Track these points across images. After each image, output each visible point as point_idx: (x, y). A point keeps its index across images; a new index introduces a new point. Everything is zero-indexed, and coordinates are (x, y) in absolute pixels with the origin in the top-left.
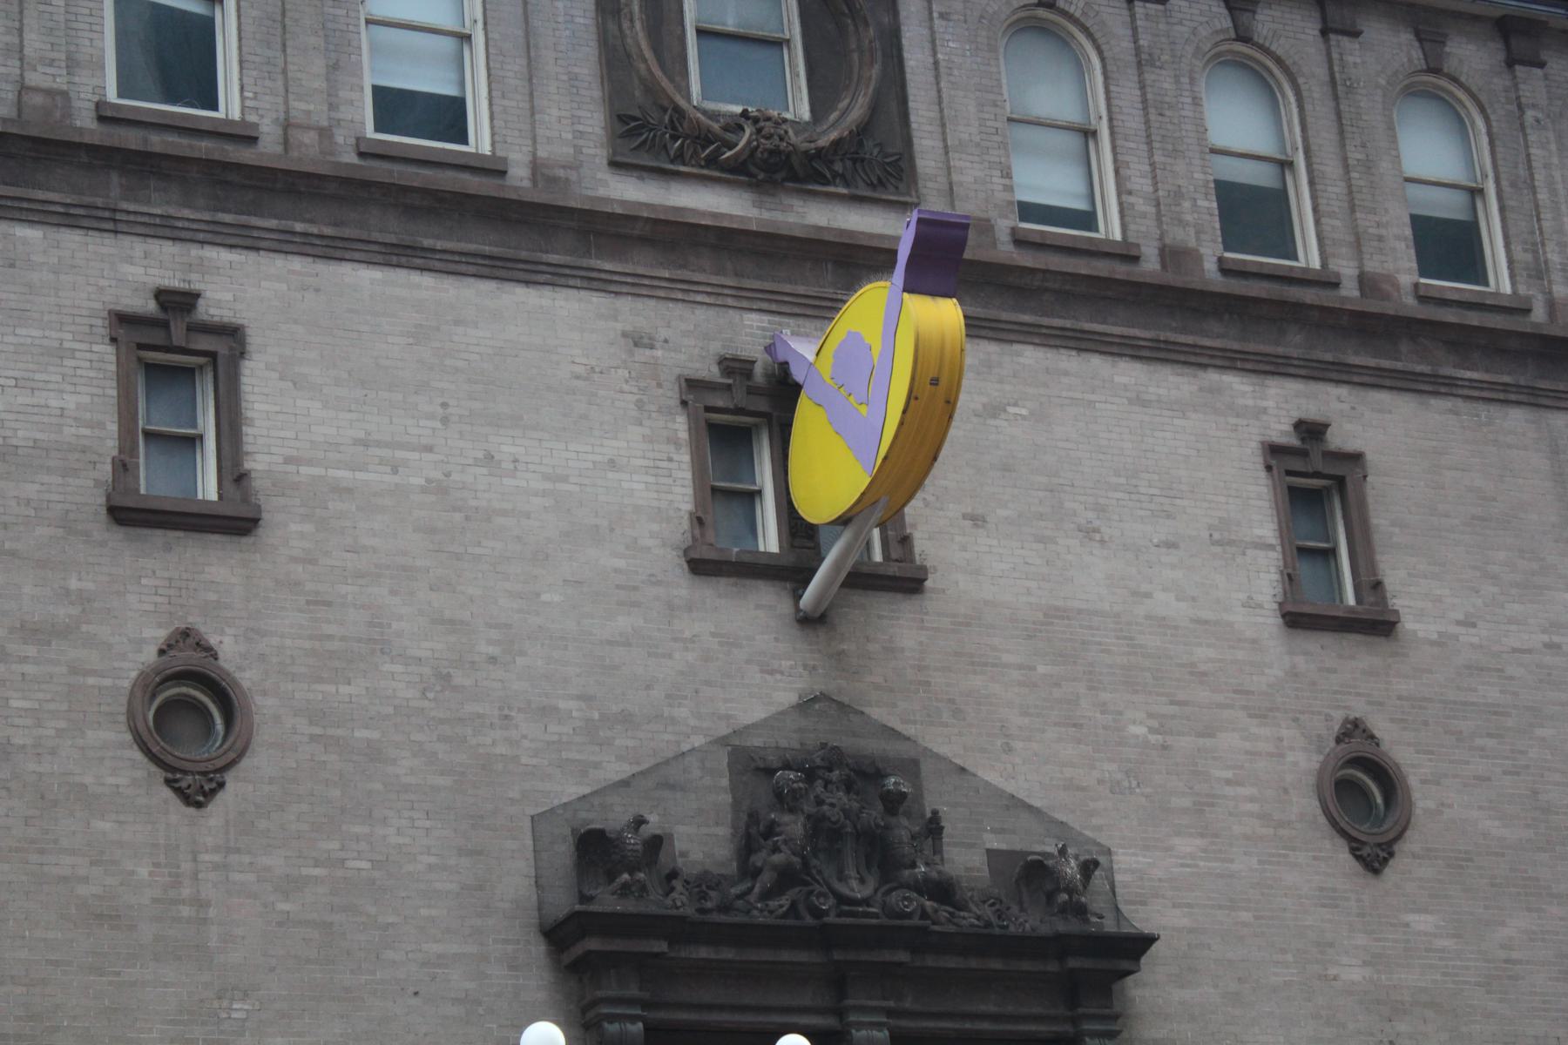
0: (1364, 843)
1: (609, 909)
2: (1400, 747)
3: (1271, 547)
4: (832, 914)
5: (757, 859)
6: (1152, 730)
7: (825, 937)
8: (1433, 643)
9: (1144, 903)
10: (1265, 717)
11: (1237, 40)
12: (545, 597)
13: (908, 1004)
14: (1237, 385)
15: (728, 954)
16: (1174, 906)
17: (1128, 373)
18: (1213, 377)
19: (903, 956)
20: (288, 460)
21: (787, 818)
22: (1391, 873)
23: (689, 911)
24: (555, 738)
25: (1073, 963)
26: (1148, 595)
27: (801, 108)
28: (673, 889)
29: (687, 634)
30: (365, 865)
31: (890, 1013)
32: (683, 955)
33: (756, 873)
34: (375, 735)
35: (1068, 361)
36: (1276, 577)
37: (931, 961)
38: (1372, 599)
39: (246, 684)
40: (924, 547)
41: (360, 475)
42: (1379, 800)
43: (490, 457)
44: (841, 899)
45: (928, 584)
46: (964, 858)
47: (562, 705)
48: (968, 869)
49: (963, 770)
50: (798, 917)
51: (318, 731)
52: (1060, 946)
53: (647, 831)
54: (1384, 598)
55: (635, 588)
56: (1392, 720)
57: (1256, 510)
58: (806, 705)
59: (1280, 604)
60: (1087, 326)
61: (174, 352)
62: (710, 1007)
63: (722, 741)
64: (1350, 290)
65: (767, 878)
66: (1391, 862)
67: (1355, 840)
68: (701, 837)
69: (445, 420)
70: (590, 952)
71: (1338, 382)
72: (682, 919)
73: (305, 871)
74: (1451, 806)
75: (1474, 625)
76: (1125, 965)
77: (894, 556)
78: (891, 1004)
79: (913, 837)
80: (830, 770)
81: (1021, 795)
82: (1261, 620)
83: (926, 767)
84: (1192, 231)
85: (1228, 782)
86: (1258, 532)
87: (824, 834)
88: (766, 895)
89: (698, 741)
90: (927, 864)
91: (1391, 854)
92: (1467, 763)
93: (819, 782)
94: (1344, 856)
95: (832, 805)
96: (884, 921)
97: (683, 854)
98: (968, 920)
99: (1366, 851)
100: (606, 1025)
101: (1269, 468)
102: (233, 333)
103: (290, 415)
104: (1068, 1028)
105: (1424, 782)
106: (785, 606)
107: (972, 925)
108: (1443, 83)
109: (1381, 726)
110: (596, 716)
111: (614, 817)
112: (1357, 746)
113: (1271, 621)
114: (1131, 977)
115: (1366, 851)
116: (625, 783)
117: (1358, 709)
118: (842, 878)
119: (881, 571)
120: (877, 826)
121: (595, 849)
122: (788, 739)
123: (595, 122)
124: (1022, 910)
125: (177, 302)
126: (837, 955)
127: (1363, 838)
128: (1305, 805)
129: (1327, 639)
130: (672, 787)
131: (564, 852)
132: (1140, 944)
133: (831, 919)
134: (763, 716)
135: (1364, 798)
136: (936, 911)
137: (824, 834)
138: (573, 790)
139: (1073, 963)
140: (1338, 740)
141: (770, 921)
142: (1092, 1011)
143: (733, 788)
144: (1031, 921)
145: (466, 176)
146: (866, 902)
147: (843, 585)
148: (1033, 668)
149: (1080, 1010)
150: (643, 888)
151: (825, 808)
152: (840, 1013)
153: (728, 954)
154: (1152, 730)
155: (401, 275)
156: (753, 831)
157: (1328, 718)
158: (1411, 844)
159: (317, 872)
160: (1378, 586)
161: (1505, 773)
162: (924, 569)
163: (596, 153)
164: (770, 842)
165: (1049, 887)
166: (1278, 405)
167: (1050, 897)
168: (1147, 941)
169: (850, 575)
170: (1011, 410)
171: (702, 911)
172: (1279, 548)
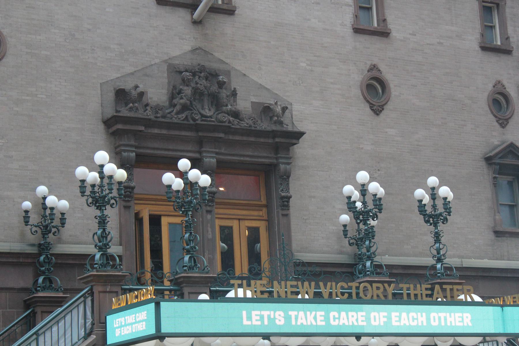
0: (374, 105)
1: (125, 115)
2: (388, 74)
3: (350, 6)
4: (199, 120)
5: (175, 101)
6: (308, 65)
7: (197, 128)
8: (401, 41)
9: (301, 121)
10: (345, 62)
12: (107, 10)
13: (223, 151)
15: (164, 132)
16: (311, 123)
19: (222, 135)
21: (185, 88)
22: (382, 115)
23: (152, 117)
24: (109, 57)
25: (277, 140)
26: (309, 20)
28: (147, 110)
29: (155, 25)
30: (44, 96)
31: (217, 153)
32: (149, 131)
33: (175, 106)
34: (49, 53)
36: (352, 16)
37: (231, 137)
38: (382, 25)
39: (5, 34)
42: (380, 91)
44: (202, 116)
45: (236, 12)
46: (244, 104)
47: (112, 46)
48: (244, 108)
49: (245, 75)
50: (188, 121)
51: (29, 51)
52: (274, 134)
53: (139, 90)
54: (387, 25)
55: (138, 8)
56: (386, 65)
58: (194, 50)
59: (352, 25)
62: (158, 149)
63: (165, 61)
65: (178, 107)
66: (383, 112)
67: (372, 104)
68: (157, 93)
70: (118, 129)
72: (150, 119)
73: (23, 98)
74: (403, 94)
75: (415, 35)
76: (294, 141)
77: (225, 2)
78: (217, 150)
79: (227, 96)
80: (201, 73)
81: (263, 84)
82: (346, 30)
83: (233, 73)
85: (332, 83)
87: (198, 94)
88: (178, 113)
89: (157, 61)
90: (231, 105)
91: (383, 109)
92: (410, 80)
93: (197, 77)
94: (368, 109)
95: (201, 84)
96: (216, 123)
97: (151, 98)
98: (244, 124)
99: (375, 108)
100: (123, 153)
104: (275, 161)
105: (395, 86)
106: (188, 17)
107: (245, 126)
109: (382, 67)
110: (123, 51)
111: (128, 85)
112: (375, 73)
113: (349, 31)
114: (295, 146)
115: (375, 108)
116: (132, 74)
117: (375, 61)
118: (203, 108)
119: (222, 7)
120: (216, 92)
121: (121, 95)
122: (188, 62)
124: (262, 122)
126: (200, 134)
127: (374, 103)
128: (356, 92)
129: (367, 37)
130: (146, 75)
131: (111, 96)
132: (299, 135)
133: (199, 122)
134: (179, 54)
135: (376, 90)
136: (233, 121)
137: (198, 94)
138: (115, 75)
139: (277, 140)
140: (368, 71)
141: (179, 121)
142: (283, 156)
143: (168, 77)
144: (265, 125)
146: (211, 117)
147: (208, 11)
148: (269, 42)
149: (279, 155)
150: (137, 109)
151: (199, 85)
152: (200, 153)
153: (164, 132)
154: (308, 65)
156: (174, 92)
157: (366, 63)
158: (389, 107)
159: (27, 98)
160: (385, 20)
161: (422, 84)
162: (235, 7)
164: (180, 96)
165: (271, 115)
167: (271, 118)
168: (301, 134)
169: (210, 8)
171: (156, 117)
172: (353, 6)
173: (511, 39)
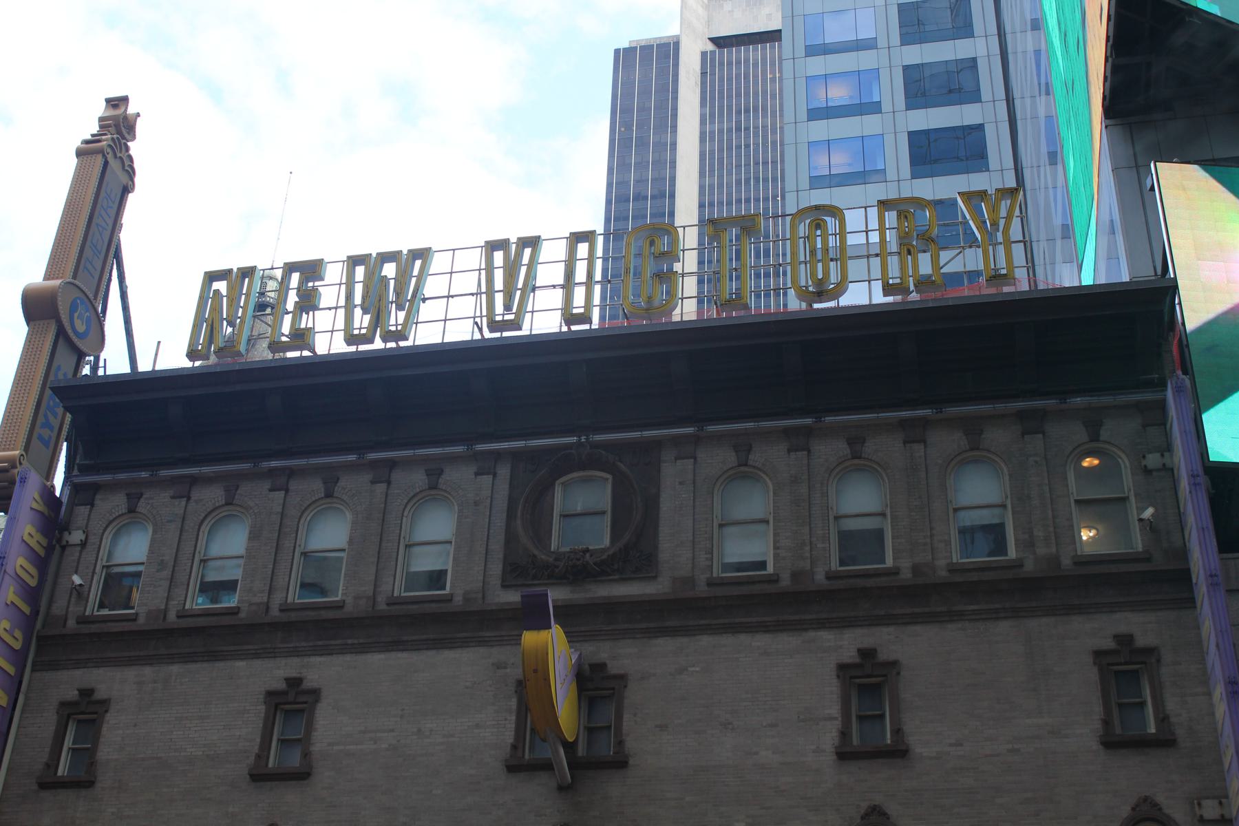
3: (836, 719)
11: (853, 458)
14: (826, 637)
17: (761, 641)
18: (812, 634)
20: (329, 744)
26: (756, 753)
27: (607, 541)
35: (727, 640)
40: (631, 744)
41: (359, 747)
43: (419, 730)
45: (631, 762)
57: (826, 697)
60: (737, 620)
61: (292, 704)
64: (906, 575)
69: (402, 717)
71: (888, 625)
75: (961, 745)
84: (809, 561)
86: (827, 712)
101: (838, 677)
102: (315, 694)
103: (330, 727)
108: (985, 454)
113: (829, 757)
123: (496, 569)
125: (294, 683)
140: (862, 818)
145: (433, 605)
155: (393, 655)
163: (495, 581)
166: (846, 644)
170: (691, 669)
173: (1173, 720)
